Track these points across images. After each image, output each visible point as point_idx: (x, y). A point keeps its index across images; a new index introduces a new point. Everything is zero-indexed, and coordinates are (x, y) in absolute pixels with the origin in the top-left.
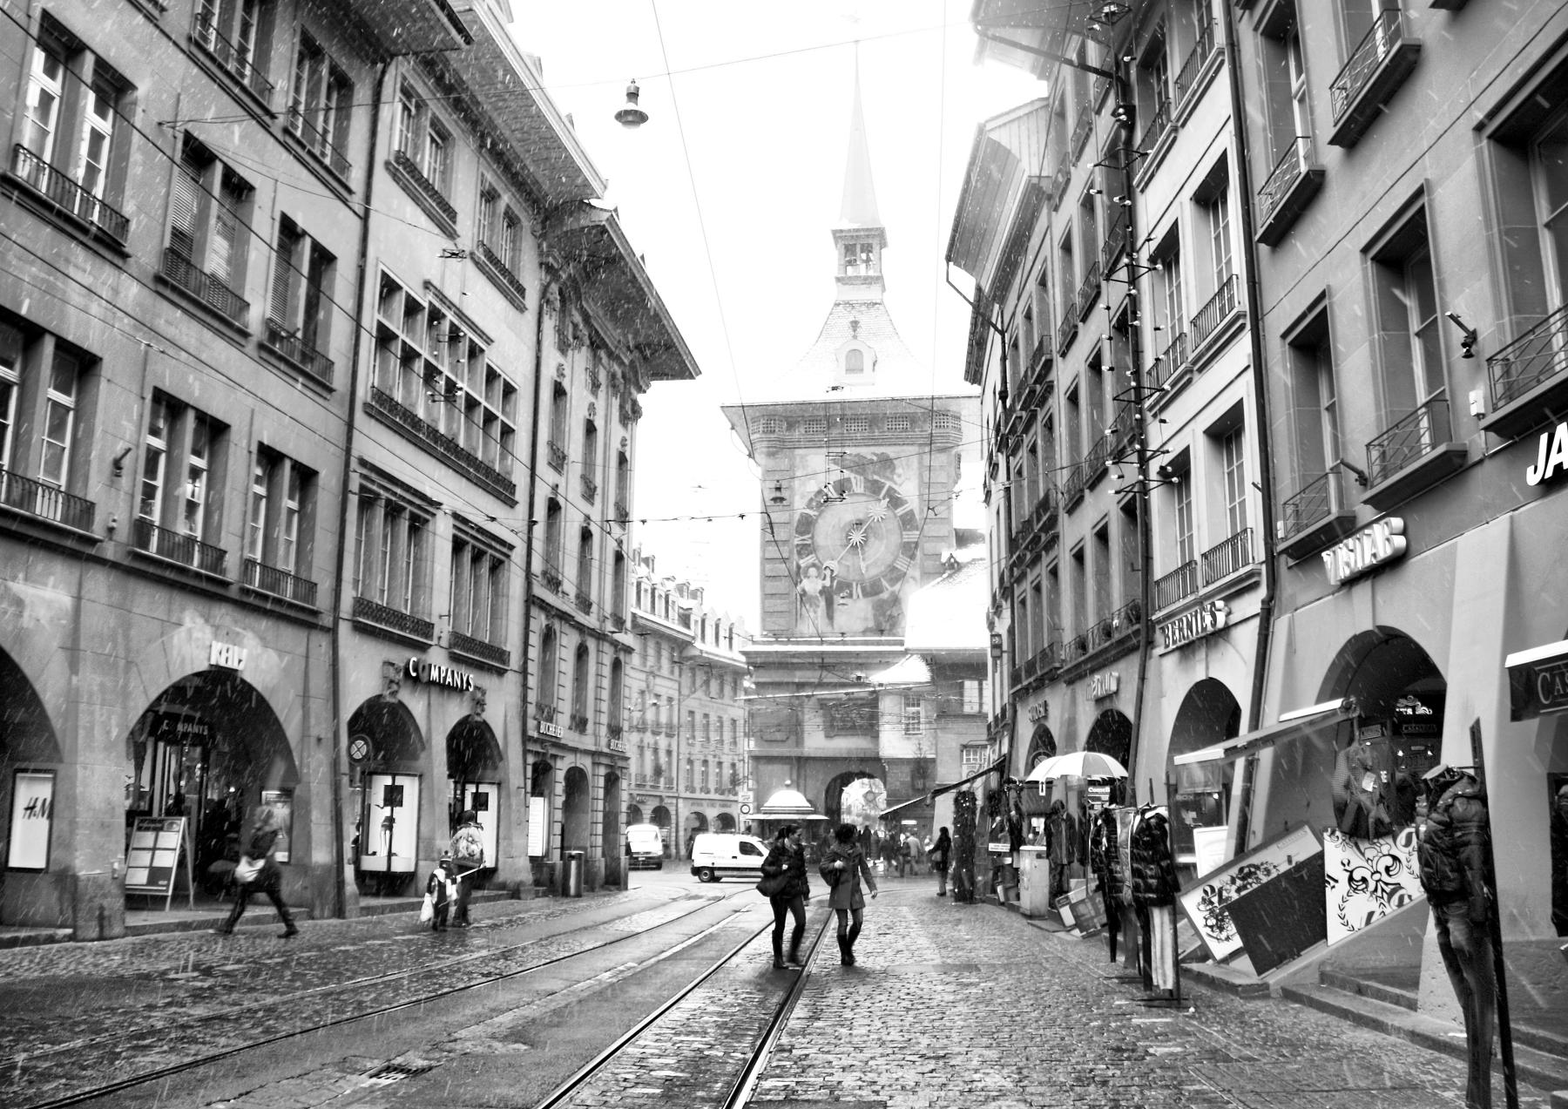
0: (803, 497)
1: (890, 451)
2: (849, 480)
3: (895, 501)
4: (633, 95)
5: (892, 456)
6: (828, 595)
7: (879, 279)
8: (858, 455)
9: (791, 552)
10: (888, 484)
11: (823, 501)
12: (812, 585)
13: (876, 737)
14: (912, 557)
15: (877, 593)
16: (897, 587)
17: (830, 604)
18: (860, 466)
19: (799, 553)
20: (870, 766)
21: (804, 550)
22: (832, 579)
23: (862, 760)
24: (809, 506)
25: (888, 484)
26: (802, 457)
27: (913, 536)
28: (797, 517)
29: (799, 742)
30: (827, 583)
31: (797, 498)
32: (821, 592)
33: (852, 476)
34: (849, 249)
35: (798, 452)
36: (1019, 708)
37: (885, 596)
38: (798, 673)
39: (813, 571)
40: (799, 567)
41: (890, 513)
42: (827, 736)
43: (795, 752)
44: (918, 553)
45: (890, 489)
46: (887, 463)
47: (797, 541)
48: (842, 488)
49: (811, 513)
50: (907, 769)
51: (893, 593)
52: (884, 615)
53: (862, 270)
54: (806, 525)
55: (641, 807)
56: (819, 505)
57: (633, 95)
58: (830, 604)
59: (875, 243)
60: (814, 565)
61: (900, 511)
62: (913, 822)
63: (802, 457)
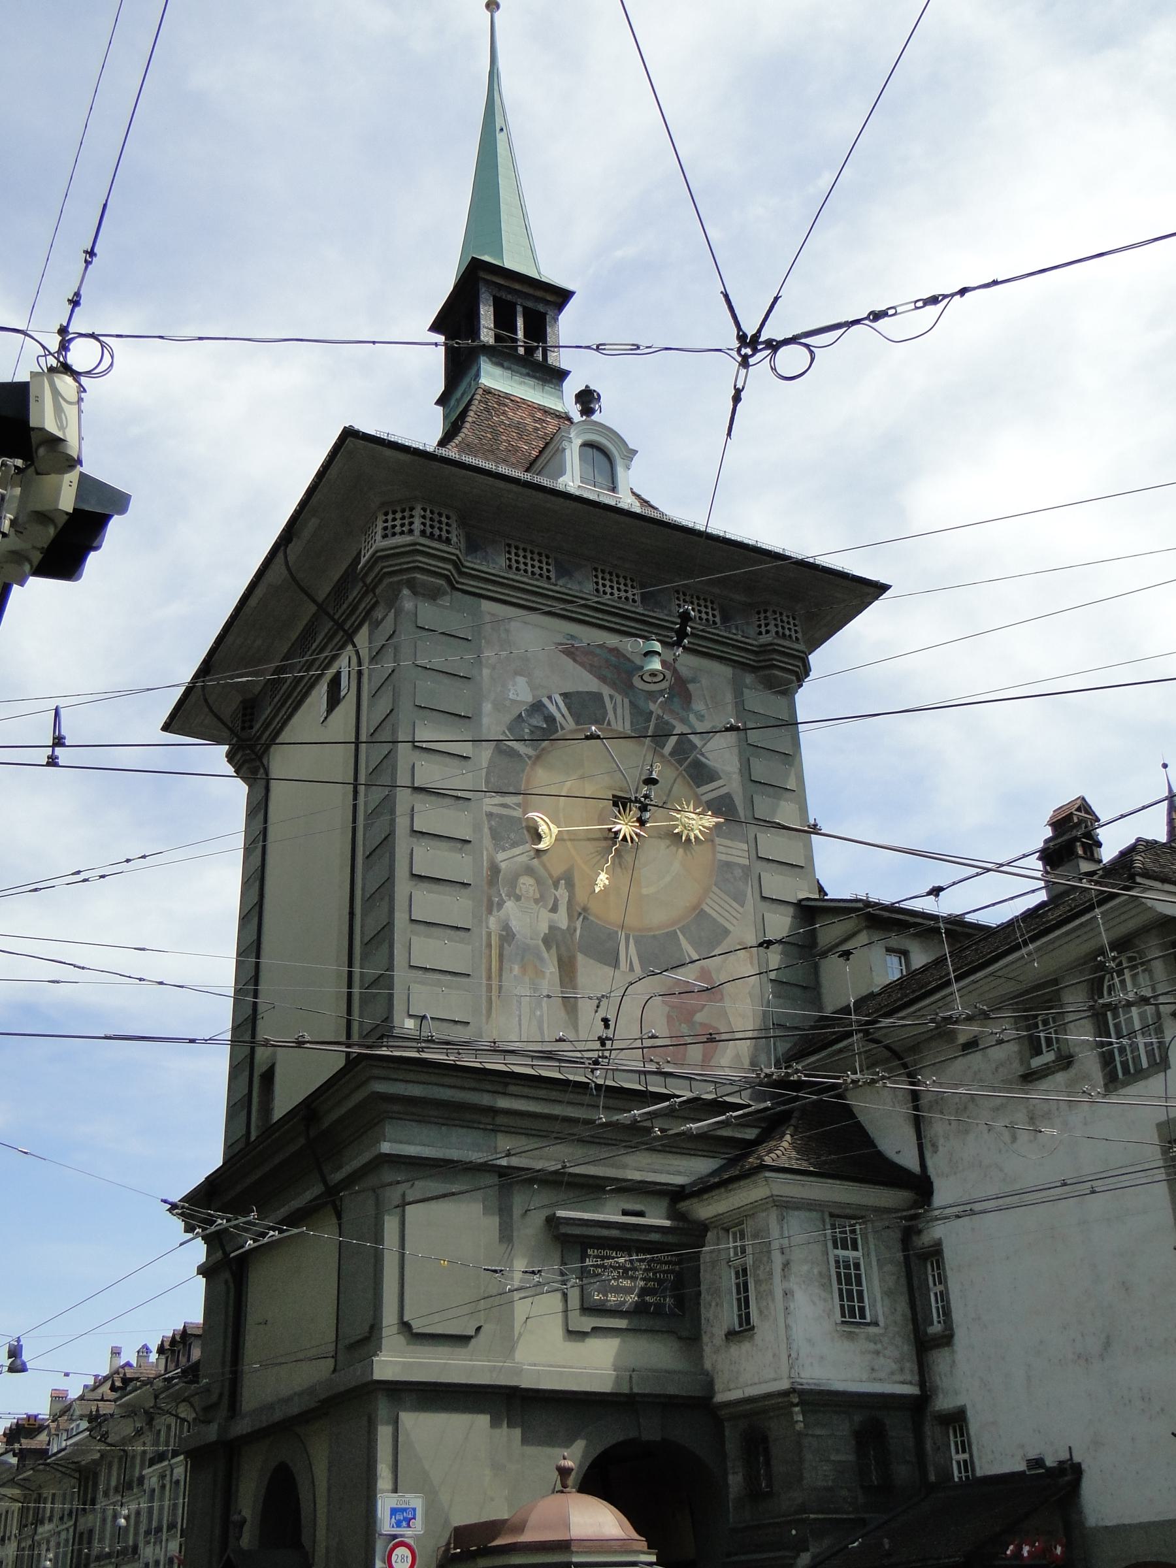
0: (498, 707)
2: (598, 697)
6: (566, 952)
8: (615, 651)
9: (477, 828)
12: (526, 918)
17: (567, 969)
19: (495, 836)
23: (667, 1404)
25: (680, 728)
26: (497, 622)
30: (562, 919)
31: (487, 707)
32: (547, 941)
33: (606, 691)
35: (486, 605)
38: (504, 1143)
39: (526, 884)
40: (495, 870)
50: (842, 1428)
58: (567, 969)
60: (529, 871)
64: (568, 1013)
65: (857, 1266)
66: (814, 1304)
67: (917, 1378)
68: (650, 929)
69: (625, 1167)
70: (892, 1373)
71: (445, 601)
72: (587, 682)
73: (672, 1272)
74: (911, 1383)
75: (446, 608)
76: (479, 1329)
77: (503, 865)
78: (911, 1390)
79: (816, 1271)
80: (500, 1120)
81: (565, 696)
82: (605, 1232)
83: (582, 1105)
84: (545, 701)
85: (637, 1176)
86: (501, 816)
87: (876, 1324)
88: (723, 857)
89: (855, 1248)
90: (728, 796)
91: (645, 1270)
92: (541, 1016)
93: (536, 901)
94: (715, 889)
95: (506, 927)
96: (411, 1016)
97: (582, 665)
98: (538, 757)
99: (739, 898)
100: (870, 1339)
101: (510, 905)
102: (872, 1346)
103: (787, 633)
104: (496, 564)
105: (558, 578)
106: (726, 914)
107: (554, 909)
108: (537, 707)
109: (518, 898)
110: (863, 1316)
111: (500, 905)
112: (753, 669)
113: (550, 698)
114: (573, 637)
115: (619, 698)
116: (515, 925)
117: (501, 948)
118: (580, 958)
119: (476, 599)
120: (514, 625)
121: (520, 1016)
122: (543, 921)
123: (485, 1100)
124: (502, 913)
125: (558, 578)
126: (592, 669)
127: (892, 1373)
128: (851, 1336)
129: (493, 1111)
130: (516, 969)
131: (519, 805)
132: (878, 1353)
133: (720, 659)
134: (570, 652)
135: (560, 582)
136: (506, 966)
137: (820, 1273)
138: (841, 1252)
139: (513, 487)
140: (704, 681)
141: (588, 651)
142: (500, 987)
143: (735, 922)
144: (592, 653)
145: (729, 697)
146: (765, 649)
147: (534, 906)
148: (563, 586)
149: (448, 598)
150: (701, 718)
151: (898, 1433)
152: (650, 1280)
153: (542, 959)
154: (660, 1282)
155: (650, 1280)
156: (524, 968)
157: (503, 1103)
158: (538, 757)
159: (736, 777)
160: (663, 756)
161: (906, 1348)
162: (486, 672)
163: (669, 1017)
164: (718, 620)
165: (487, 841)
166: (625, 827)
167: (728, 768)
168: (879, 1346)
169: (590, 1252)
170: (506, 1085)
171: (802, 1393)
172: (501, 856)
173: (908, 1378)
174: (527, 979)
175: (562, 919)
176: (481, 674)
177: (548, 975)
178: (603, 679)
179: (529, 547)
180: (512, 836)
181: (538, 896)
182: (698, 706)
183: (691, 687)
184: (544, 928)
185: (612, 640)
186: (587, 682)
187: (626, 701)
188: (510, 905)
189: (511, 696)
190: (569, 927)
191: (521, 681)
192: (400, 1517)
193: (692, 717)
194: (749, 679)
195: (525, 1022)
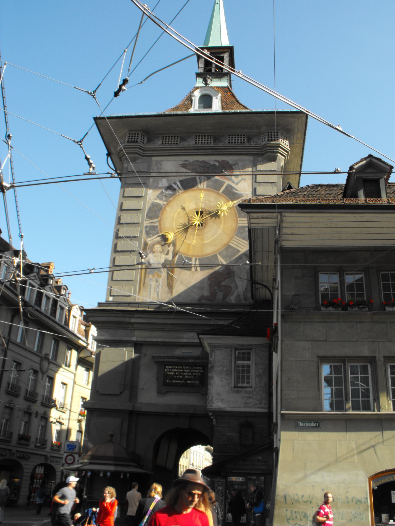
5: (231, 162)
8: (204, 162)
9: (141, 232)
10: (227, 182)
22: (174, 255)
23: (193, 416)
25: (227, 182)
30: (170, 257)
35: (154, 159)
38: (137, 333)
40: (146, 244)
42: (160, 392)
43: (127, 406)
45: (229, 187)
47: (147, 223)
49: (161, 202)
55: (23, 463)
62: (240, 479)
63: (158, 163)
64: (169, 288)
65: (249, 366)
66: (222, 381)
67: (267, 406)
68: (206, 255)
69: (183, 338)
70: (256, 405)
71: (139, 161)
73: (199, 372)
74: (264, 408)
75: (139, 163)
76: (121, 393)
77: (149, 243)
78: (265, 410)
79: (225, 369)
80: (135, 326)
81: (181, 181)
82: (171, 360)
83: (170, 318)
84: (173, 185)
85: (185, 341)
86: (150, 226)
87: (251, 387)
88: (241, 225)
89: (249, 359)
91: (189, 372)
92: (159, 290)
93: (161, 252)
94: (236, 237)
96: (111, 296)
98: (167, 204)
100: (246, 392)
101: (150, 256)
102: (248, 395)
105: (180, 143)
107: (167, 254)
109: (154, 252)
112: (262, 155)
113: (175, 183)
114: (186, 161)
116: (151, 262)
119: (149, 158)
120: (163, 163)
121: (150, 292)
122: (162, 259)
123: (127, 320)
124: (147, 259)
125: (180, 143)
127: (256, 405)
128: (238, 392)
129: (133, 324)
131: (158, 221)
132: (250, 397)
133: (248, 154)
134: (184, 166)
135: (181, 144)
136: (147, 275)
137: (227, 370)
138: (241, 362)
139: (150, 119)
141: (193, 164)
142: (144, 283)
143: (243, 247)
146: (265, 146)
147: (160, 254)
148: (186, 144)
149: (140, 160)
152: (190, 375)
154: (194, 376)
155: (190, 375)
156: (154, 276)
157: (133, 320)
158: (167, 204)
160: (219, 194)
161: (264, 395)
163: (210, 285)
164: (245, 141)
165: (144, 235)
167: (247, 192)
168: (251, 395)
169: (167, 367)
170: (133, 314)
174: (154, 279)
175: (170, 257)
176: (149, 181)
177: (162, 276)
178: (197, 172)
180: (154, 232)
181: (161, 250)
184: (162, 261)
188: (150, 256)
190: (172, 260)
192: (70, 447)
195: (152, 293)
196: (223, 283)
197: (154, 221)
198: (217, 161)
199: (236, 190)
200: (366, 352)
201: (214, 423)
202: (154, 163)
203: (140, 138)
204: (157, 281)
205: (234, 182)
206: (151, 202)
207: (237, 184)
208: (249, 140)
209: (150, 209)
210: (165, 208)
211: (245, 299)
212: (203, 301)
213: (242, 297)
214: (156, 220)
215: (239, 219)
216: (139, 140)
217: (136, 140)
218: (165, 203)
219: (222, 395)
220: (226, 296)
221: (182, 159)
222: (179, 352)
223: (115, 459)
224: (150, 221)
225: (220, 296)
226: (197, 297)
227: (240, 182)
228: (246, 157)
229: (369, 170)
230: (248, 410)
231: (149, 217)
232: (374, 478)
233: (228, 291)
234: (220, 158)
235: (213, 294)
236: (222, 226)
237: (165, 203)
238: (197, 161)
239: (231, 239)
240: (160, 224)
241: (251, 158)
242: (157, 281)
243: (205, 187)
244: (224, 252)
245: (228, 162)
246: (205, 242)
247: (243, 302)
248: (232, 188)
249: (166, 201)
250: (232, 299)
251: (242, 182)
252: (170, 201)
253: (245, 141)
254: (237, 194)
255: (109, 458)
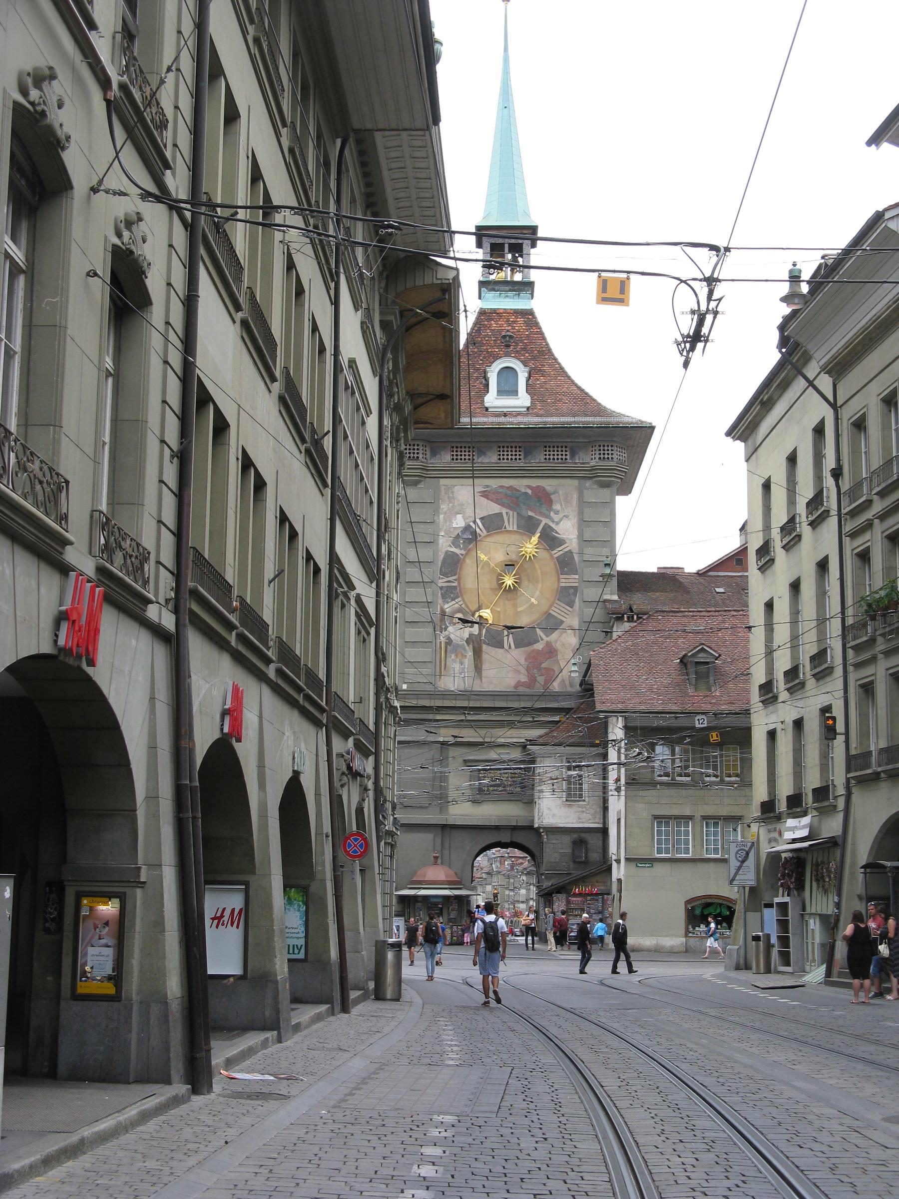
1: (547, 484)
3: (550, 540)
4: (794, 265)
5: (549, 489)
6: (476, 645)
7: (527, 286)
8: (510, 488)
9: (434, 594)
10: (544, 521)
11: (470, 538)
13: (530, 802)
14: (571, 604)
15: (530, 644)
16: (555, 635)
17: (478, 653)
18: (513, 500)
19: (444, 597)
20: (523, 838)
21: (450, 593)
23: (514, 828)
24: (455, 543)
27: (572, 580)
28: (441, 556)
29: (443, 808)
32: (467, 641)
33: (504, 511)
34: (496, 249)
36: (854, 790)
37: (539, 646)
40: (443, 613)
41: (544, 554)
44: (577, 600)
45: (547, 526)
46: (544, 499)
47: (442, 582)
48: (493, 524)
50: (567, 840)
51: (548, 644)
52: (538, 668)
53: (505, 274)
54: (452, 565)
56: (470, 541)
57: (794, 265)
58: (478, 653)
59: (526, 244)
61: (557, 552)
63: (449, 488)
72: (494, 508)
78: (601, 826)
88: (563, 585)
90: (570, 552)
95: (449, 638)
97: (492, 500)
99: (571, 604)
100: (579, 806)
103: (606, 456)
104: (445, 458)
105: (478, 458)
106: (563, 614)
108: (467, 528)
110: (581, 796)
111: (445, 630)
114: (488, 486)
115: (511, 513)
116: (452, 636)
117: (446, 648)
118: (484, 646)
123: (431, 717)
126: (497, 501)
130: (453, 656)
134: (485, 494)
140: (560, 492)
144: (498, 493)
145: (575, 496)
146: (593, 469)
150: (557, 512)
151: (594, 841)
153: (465, 649)
156: (457, 656)
157: (438, 717)
159: (575, 541)
161: (598, 810)
162: (441, 516)
165: (440, 601)
166: (509, 581)
171: (544, 828)
172: (446, 606)
173: (597, 821)
178: (503, 505)
179: (463, 445)
182: (557, 507)
183: (553, 497)
184: (467, 635)
185: (507, 482)
186: (494, 508)
187: (515, 513)
189: (454, 526)
191: (459, 516)
193: (552, 514)
194: (588, 483)
196: (543, 665)
197: (449, 579)
198: (529, 487)
199: (557, 532)
200: (688, 813)
201: (545, 840)
202: (443, 488)
203: (421, 452)
204: (461, 663)
205: (553, 522)
206: (444, 551)
207: (557, 523)
208: (573, 455)
209: (444, 561)
210: (464, 560)
211: (571, 686)
212: (521, 689)
213: (567, 683)
214: (454, 578)
215: (561, 576)
216: (421, 456)
217: (416, 455)
218: (463, 552)
219: (552, 810)
220: (548, 681)
221: (481, 484)
222: (493, 755)
223: (449, 882)
224: (446, 579)
225: (541, 680)
226: (513, 683)
227: (561, 520)
228: (568, 481)
229: (701, 655)
230: (581, 825)
231: (445, 575)
232: (688, 902)
233: (550, 676)
234: (534, 483)
235: (533, 680)
236: (540, 585)
237: (463, 552)
238: (502, 487)
239: (551, 606)
240: (459, 583)
241: (576, 482)
242: (461, 663)
243: (515, 529)
244: (544, 623)
245: (544, 489)
246: (519, 610)
247: (569, 689)
248: (552, 530)
249: (464, 549)
250: (556, 686)
251: (565, 521)
252: (469, 550)
253: (568, 457)
254: (558, 538)
255: (442, 882)
